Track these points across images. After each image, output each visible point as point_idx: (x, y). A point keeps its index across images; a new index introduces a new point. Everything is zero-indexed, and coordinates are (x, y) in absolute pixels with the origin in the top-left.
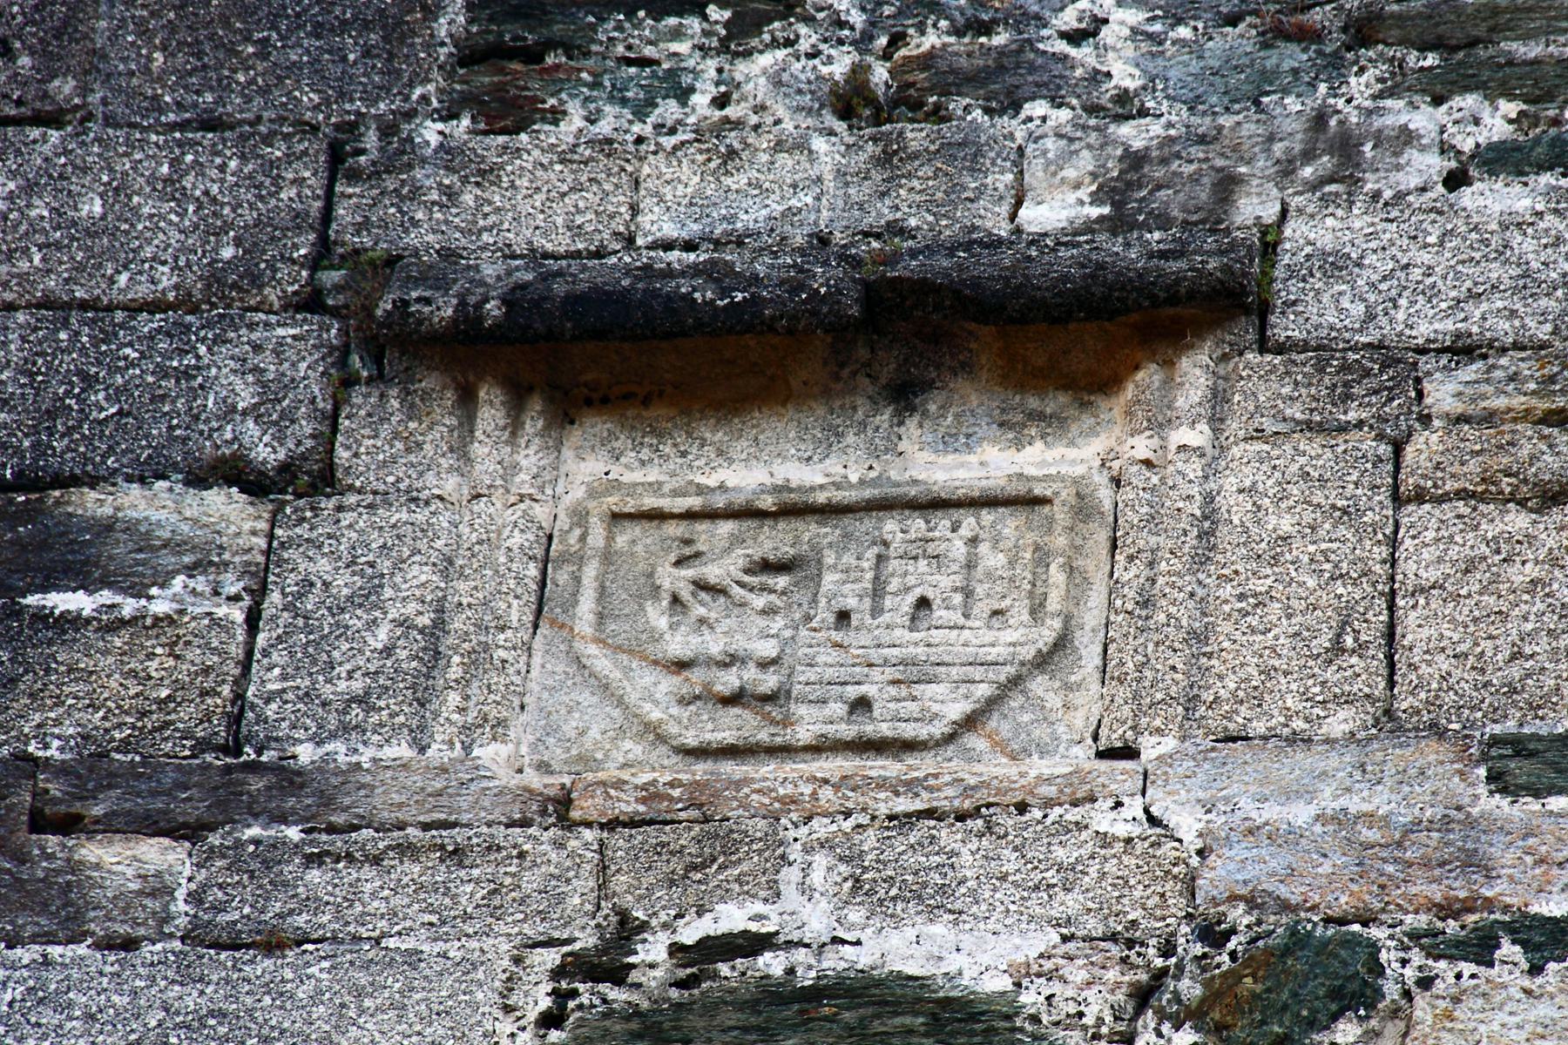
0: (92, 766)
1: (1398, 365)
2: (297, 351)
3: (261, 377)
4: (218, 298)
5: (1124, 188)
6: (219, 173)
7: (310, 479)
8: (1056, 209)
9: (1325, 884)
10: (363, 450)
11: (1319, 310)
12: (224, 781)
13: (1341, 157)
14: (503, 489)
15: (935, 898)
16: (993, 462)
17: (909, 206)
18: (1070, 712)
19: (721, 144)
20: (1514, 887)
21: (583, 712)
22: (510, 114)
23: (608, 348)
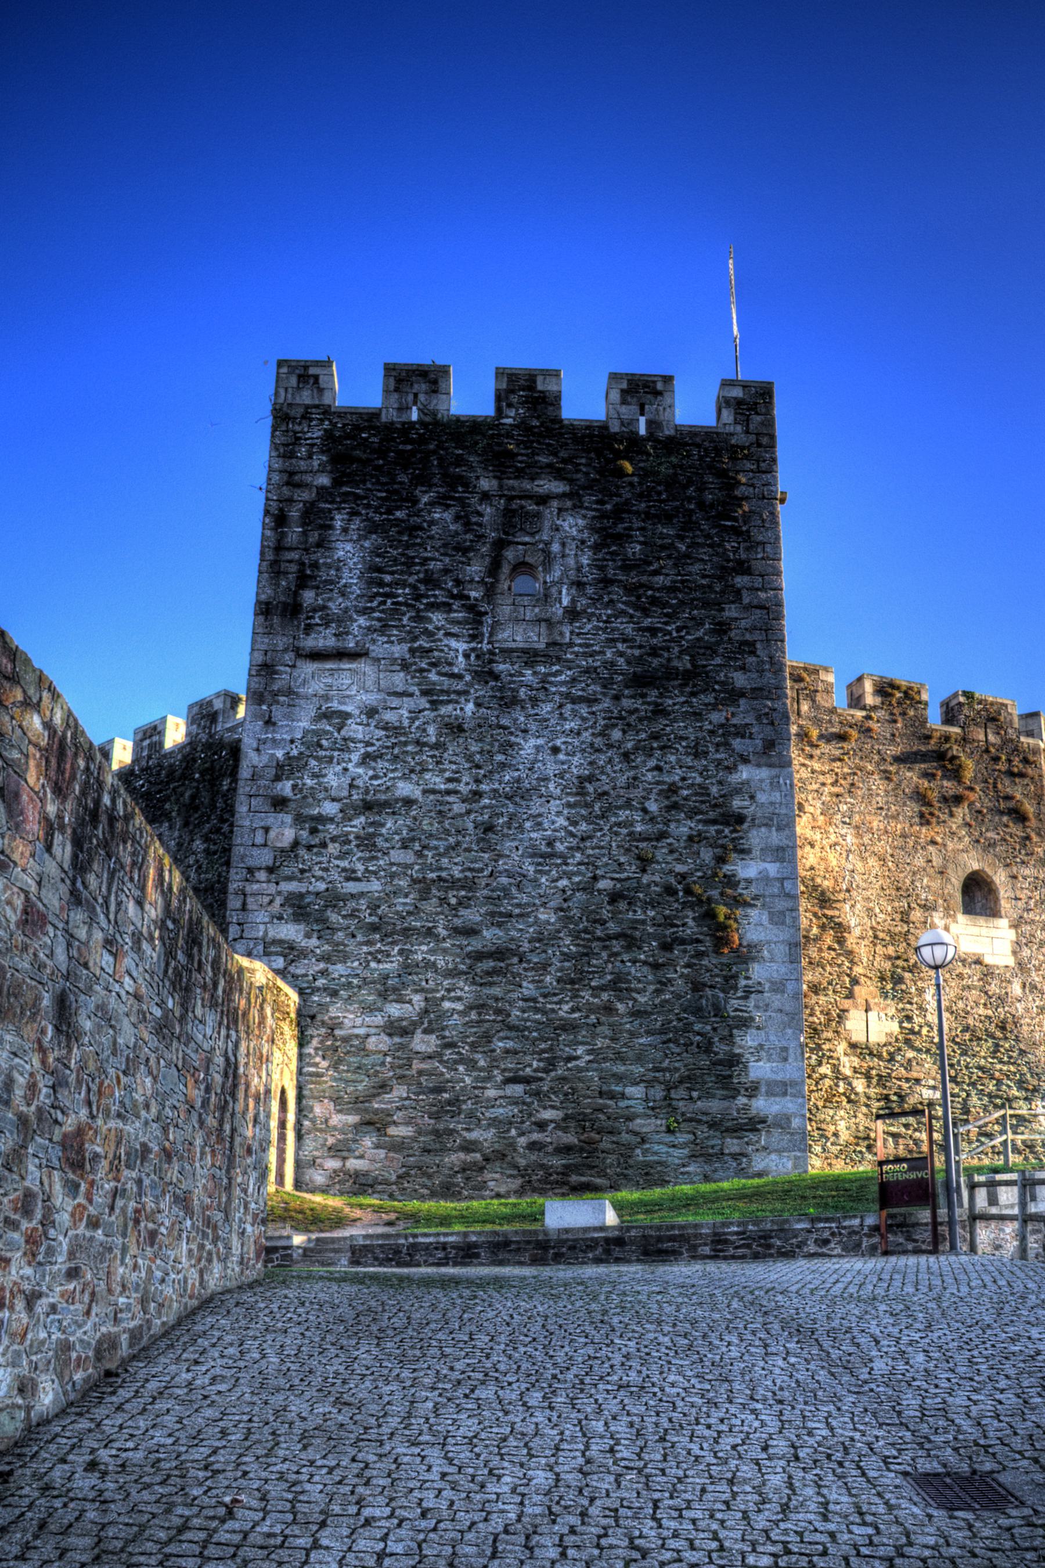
0: (279, 691)
1: (379, 660)
2: (292, 655)
3: (289, 657)
4: (285, 650)
5: (357, 643)
6: (285, 639)
7: (294, 666)
8: (351, 645)
9: (375, 703)
10: (298, 664)
11: (373, 655)
12: (290, 692)
13: (374, 641)
14: (309, 668)
15: (344, 704)
16: (347, 666)
17: (340, 644)
18: (355, 687)
19: (325, 638)
20: (388, 704)
21: (316, 687)
22: (308, 634)
23: (317, 656)
